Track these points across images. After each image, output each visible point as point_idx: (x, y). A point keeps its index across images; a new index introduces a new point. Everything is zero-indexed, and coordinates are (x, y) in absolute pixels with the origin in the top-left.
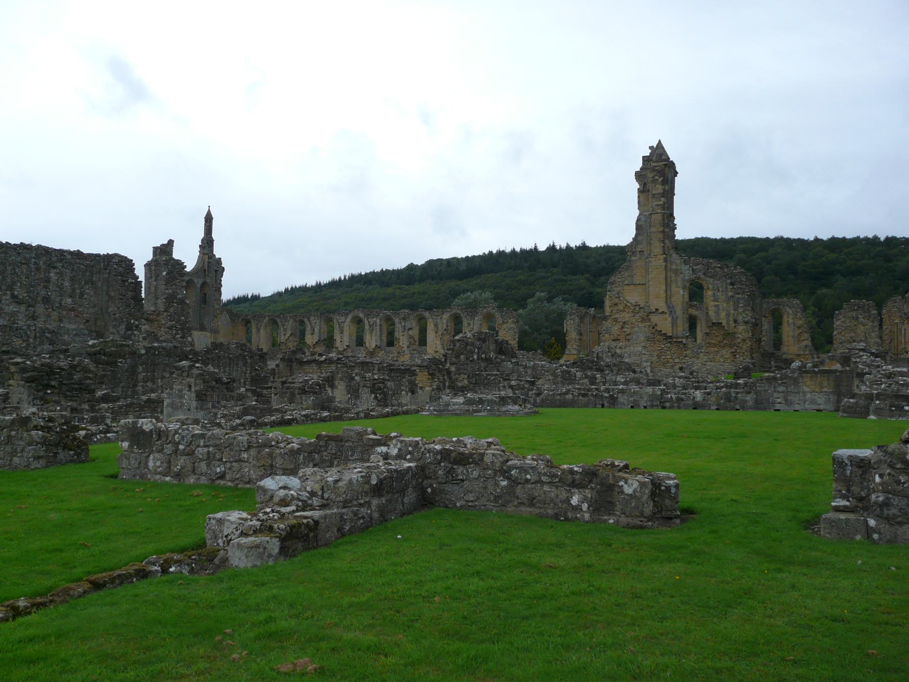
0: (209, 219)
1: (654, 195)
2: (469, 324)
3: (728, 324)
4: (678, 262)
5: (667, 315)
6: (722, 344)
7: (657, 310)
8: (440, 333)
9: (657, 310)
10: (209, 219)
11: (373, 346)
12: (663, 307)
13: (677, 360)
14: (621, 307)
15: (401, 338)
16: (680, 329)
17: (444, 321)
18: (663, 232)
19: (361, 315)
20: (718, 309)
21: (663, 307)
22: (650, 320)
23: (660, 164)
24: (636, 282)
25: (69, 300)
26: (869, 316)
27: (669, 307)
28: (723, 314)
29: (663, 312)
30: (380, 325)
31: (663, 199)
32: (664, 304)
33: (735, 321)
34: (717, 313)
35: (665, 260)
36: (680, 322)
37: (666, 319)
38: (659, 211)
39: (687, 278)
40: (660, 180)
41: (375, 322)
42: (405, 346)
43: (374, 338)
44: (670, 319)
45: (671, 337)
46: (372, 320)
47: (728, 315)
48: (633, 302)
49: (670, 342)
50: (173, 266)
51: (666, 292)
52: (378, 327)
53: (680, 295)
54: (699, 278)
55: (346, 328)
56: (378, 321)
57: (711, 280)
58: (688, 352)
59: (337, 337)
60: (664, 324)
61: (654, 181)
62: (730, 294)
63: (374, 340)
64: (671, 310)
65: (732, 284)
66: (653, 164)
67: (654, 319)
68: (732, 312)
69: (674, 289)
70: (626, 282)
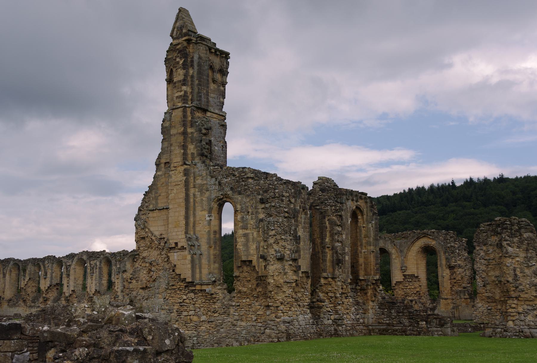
1: (175, 83)
4: (204, 173)
5: (186, 252)
6: (255, 293)
9: (176, 244)
11: (93, 290)
13: (203, 318)
15: (116, 281)
16: (205, 271)
20: (247, 240)
21: (183, 243)
23: (180, 40)
24: (160, 206)
26: (521, 242)
27: (189, 239)
29: (183, 248)
30: (100, 268)
31: (184, 88)
32: (184, 236)
34: (246, 245)
35: (186, 173)
36: (204, 261)
38: (180, 105)
39: (213, 196)
40: (181, 62)
42: (119, 290)
43: (94, 282)
44: (189, 257)
45: (192, 284)
48: (157, 233)
49: (192, 291)
51: (187, 218)
52: (97, 270)
55: (72, 272)
56: (98, 263)
58: (217, 305)
59: (65, 282)
60: (182, 261)
63: (94, 284)
64: (192, 243)
65: (262, 201)
67: (175, 257)
70: (151, 207)
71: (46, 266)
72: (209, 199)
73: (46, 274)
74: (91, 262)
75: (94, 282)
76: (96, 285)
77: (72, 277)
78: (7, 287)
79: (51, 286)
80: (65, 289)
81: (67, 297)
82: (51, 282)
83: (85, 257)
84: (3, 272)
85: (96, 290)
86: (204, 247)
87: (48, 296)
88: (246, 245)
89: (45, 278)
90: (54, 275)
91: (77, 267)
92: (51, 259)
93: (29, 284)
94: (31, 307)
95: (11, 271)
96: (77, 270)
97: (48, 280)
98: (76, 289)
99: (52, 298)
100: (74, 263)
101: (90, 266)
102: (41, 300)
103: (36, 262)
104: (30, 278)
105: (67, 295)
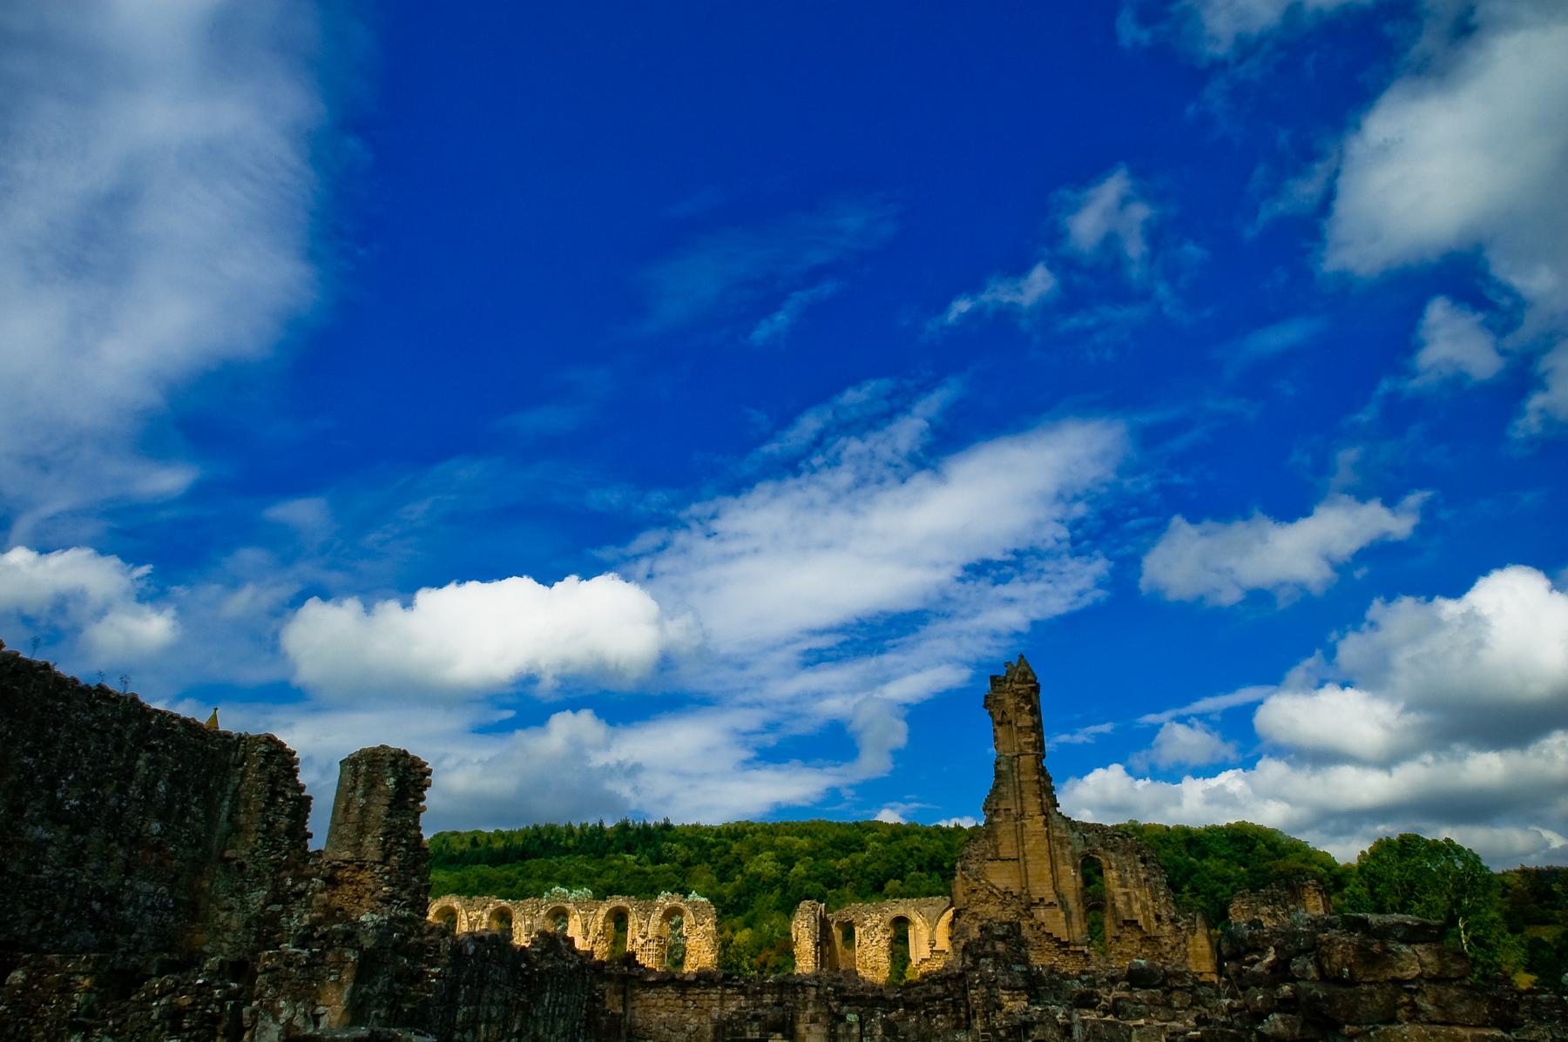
2: (641, 926)
3: (1148, 923)
7: (1042, 900)
8: (590, 939)
9: (1042, 900)
12: (1050, 897)
14: (982, 895)
16: (1077, 930)
17: (600, 920)
18: (1038, 782)
19: (456, 905)
20: (1129, 898)
21: (1050, 897)
22: (1032, 916)
25: (156, 827)
28: (1137, 907)
29: (1051, 904)
33: (1158, 918)
34: (1128, 904)
35: (1046, 824)
37: (1056, 915)
41: (480, 917)
44: (1062, 915)
45: (1066, 944)
46: (474, 915)
47: (1144, 907)
48: (1001, 887)
49: (1065, 953)
50: (406, 769)
53: (1071, 878)
54: (1094, 852)
56: (485, 916)
57: (1113, 855)
61: (1019, 709)
62: (1143, 876)
66: (1016, 686)
68: (1150, 903)
69: (1061, 868)
72: (1073, 854)
86: (1072, 905)
88: (1128, 904)
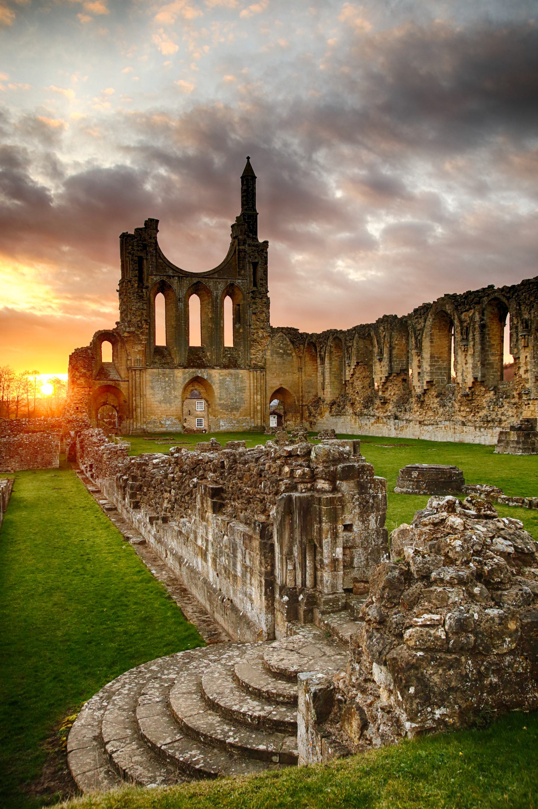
0: (249, 179)
10: (249, 179)
11: (470, 381)
30: (483, 327)
41: (472, 319)
55: (426, 343)
56: (477, 318)
63: (470, 366)
71: (382, 336)
73: (381, 353)
74: (463, 316)
75: (470, 360)
76: (474, 367)
77: (426, 354)
78: (327, 381)
79: (390, 374)
80: (415, 382)
81: (419, 397)
82: (391, 367)
83: (449, 308)
84: (320, 355)
85: (476, 379)
87: (387, 395)
89: (380, 360)
90: (395, 352)
91: (435, 332)
92: (389, 321)
93: (357, 375)
94: (361, 414)
95: (331, 352)
96: (436, 339)
97: (385, 362)
98: (436, 378)
99: (395, 398)
100: (428, 323)
101: (461, 325)
102: (378, 402)
103: (363, 332)
104: (358, 363)
105: (419, 391)
